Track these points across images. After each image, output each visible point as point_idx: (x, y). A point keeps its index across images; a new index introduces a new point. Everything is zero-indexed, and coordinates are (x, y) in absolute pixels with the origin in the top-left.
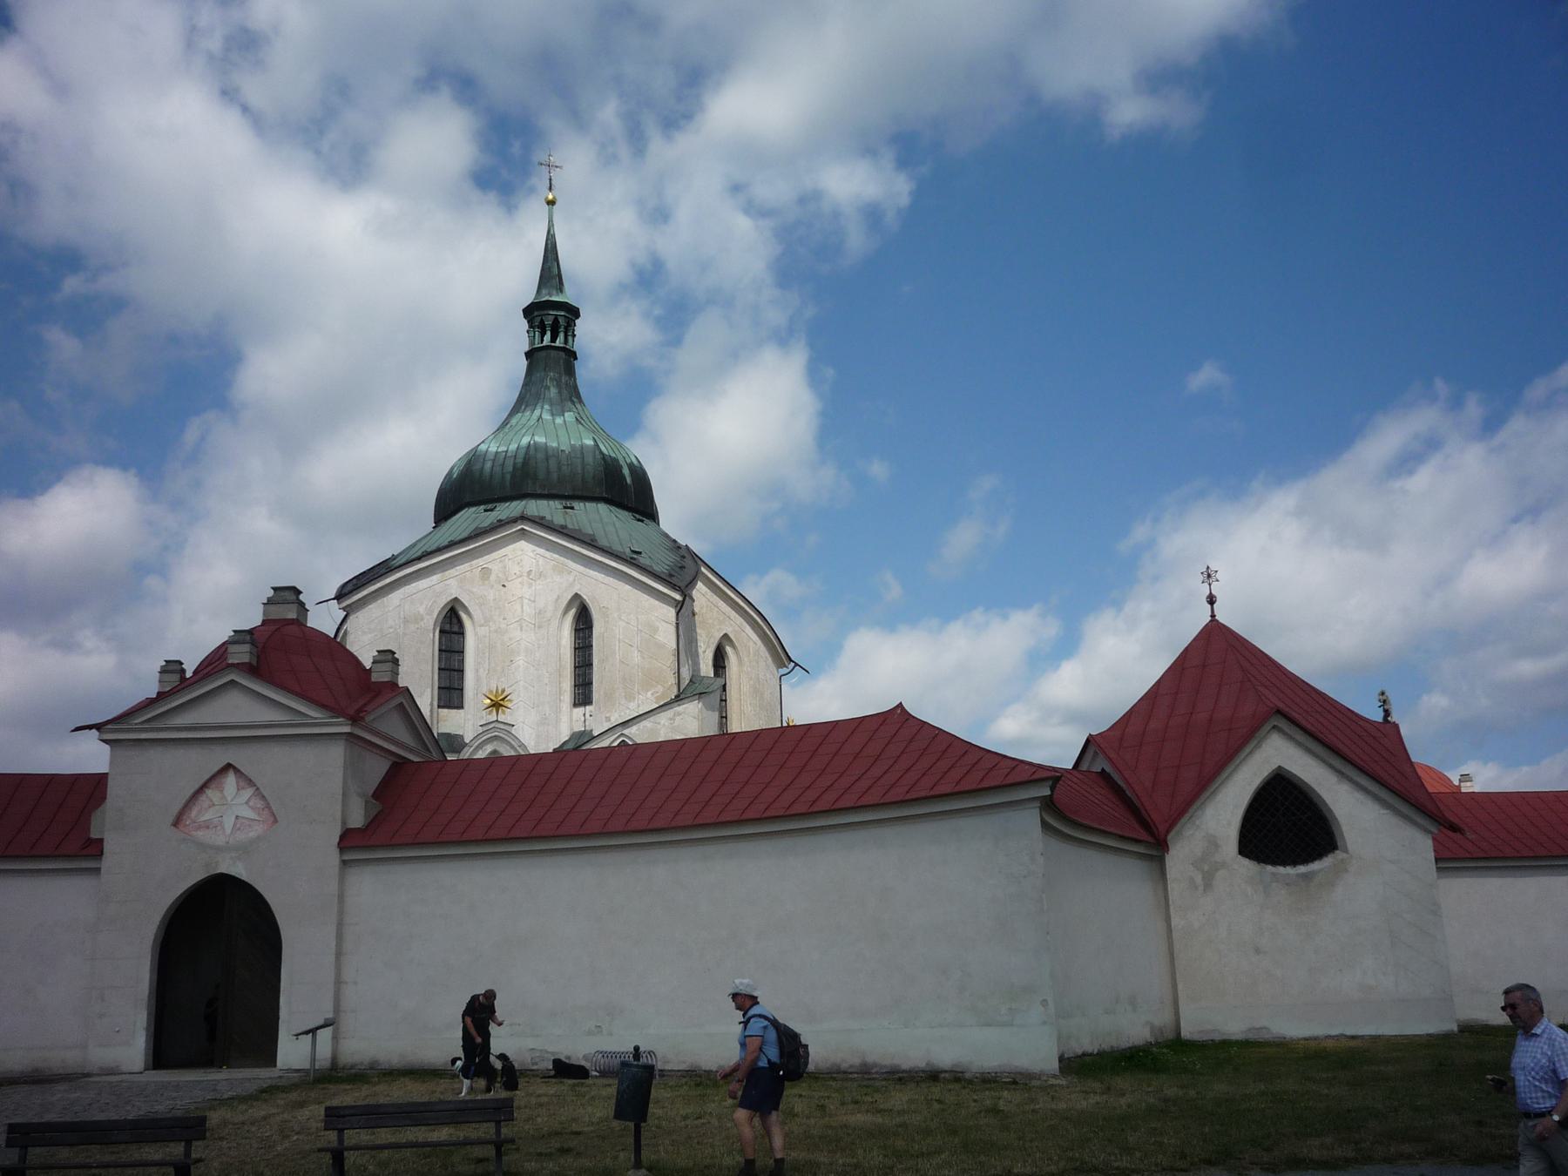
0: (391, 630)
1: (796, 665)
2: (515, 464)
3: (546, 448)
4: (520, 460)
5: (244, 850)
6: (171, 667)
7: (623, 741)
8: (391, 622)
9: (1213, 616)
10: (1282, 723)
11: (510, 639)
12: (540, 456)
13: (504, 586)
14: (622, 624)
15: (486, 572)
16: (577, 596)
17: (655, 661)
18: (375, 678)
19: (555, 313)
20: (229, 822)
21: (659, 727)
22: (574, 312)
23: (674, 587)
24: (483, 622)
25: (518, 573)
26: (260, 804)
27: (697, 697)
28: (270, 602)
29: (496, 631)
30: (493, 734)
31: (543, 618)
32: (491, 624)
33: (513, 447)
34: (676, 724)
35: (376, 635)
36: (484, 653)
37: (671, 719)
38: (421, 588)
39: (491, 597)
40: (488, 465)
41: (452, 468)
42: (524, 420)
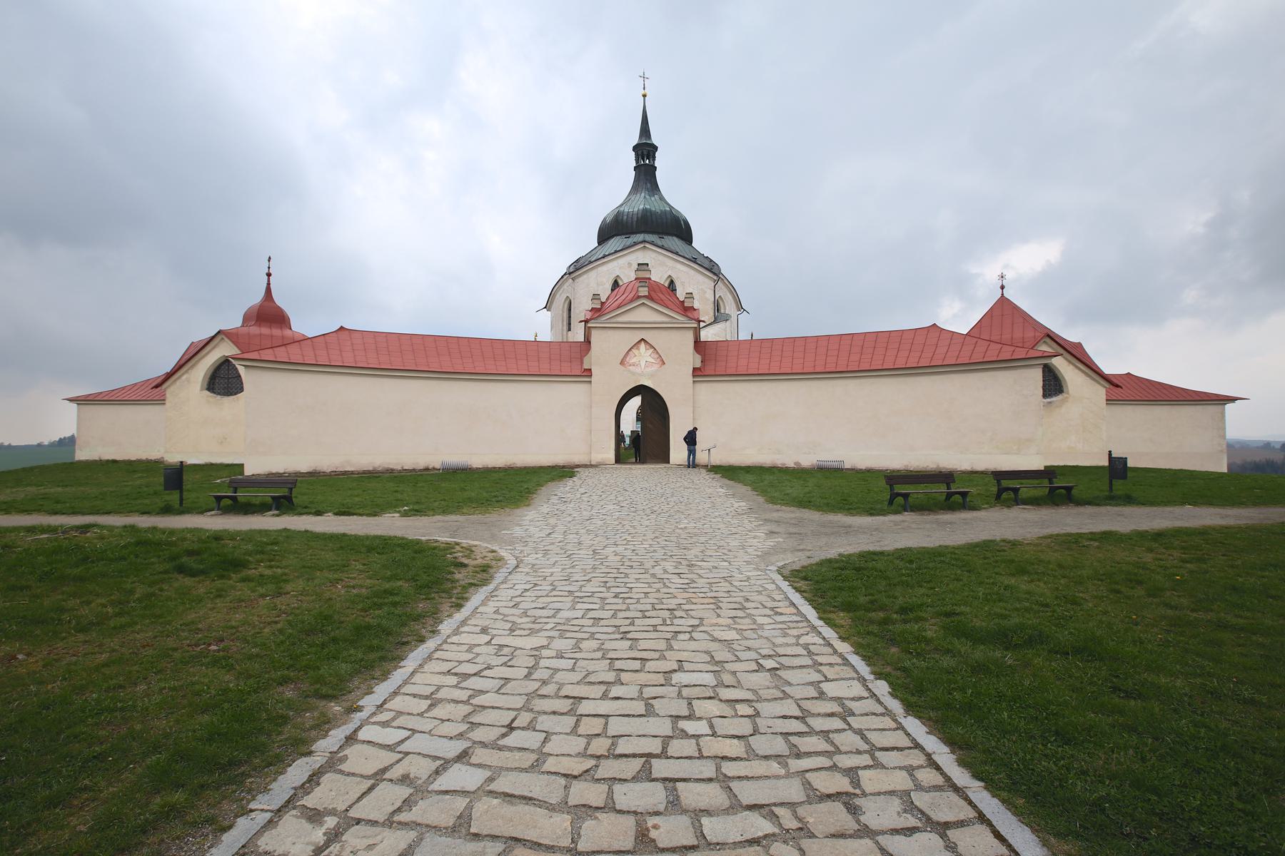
1: (744, 310)
2: (637, 218)
3: (650, 211)
4: (640, 215)
5: (652, 376)
6: (598, 297)
9: (1002, 294)
10: (1048, 340)
12: (648, 214)
16: (670, 276)
18: (686, 304)
20: (643, 364)
22: (656, 148)
23: (715, 274)
26: (656, 356)
28: (637, 270)
33: (636, 209)
40: (625, 217)
41: (605, 219)
42: (637, 198)
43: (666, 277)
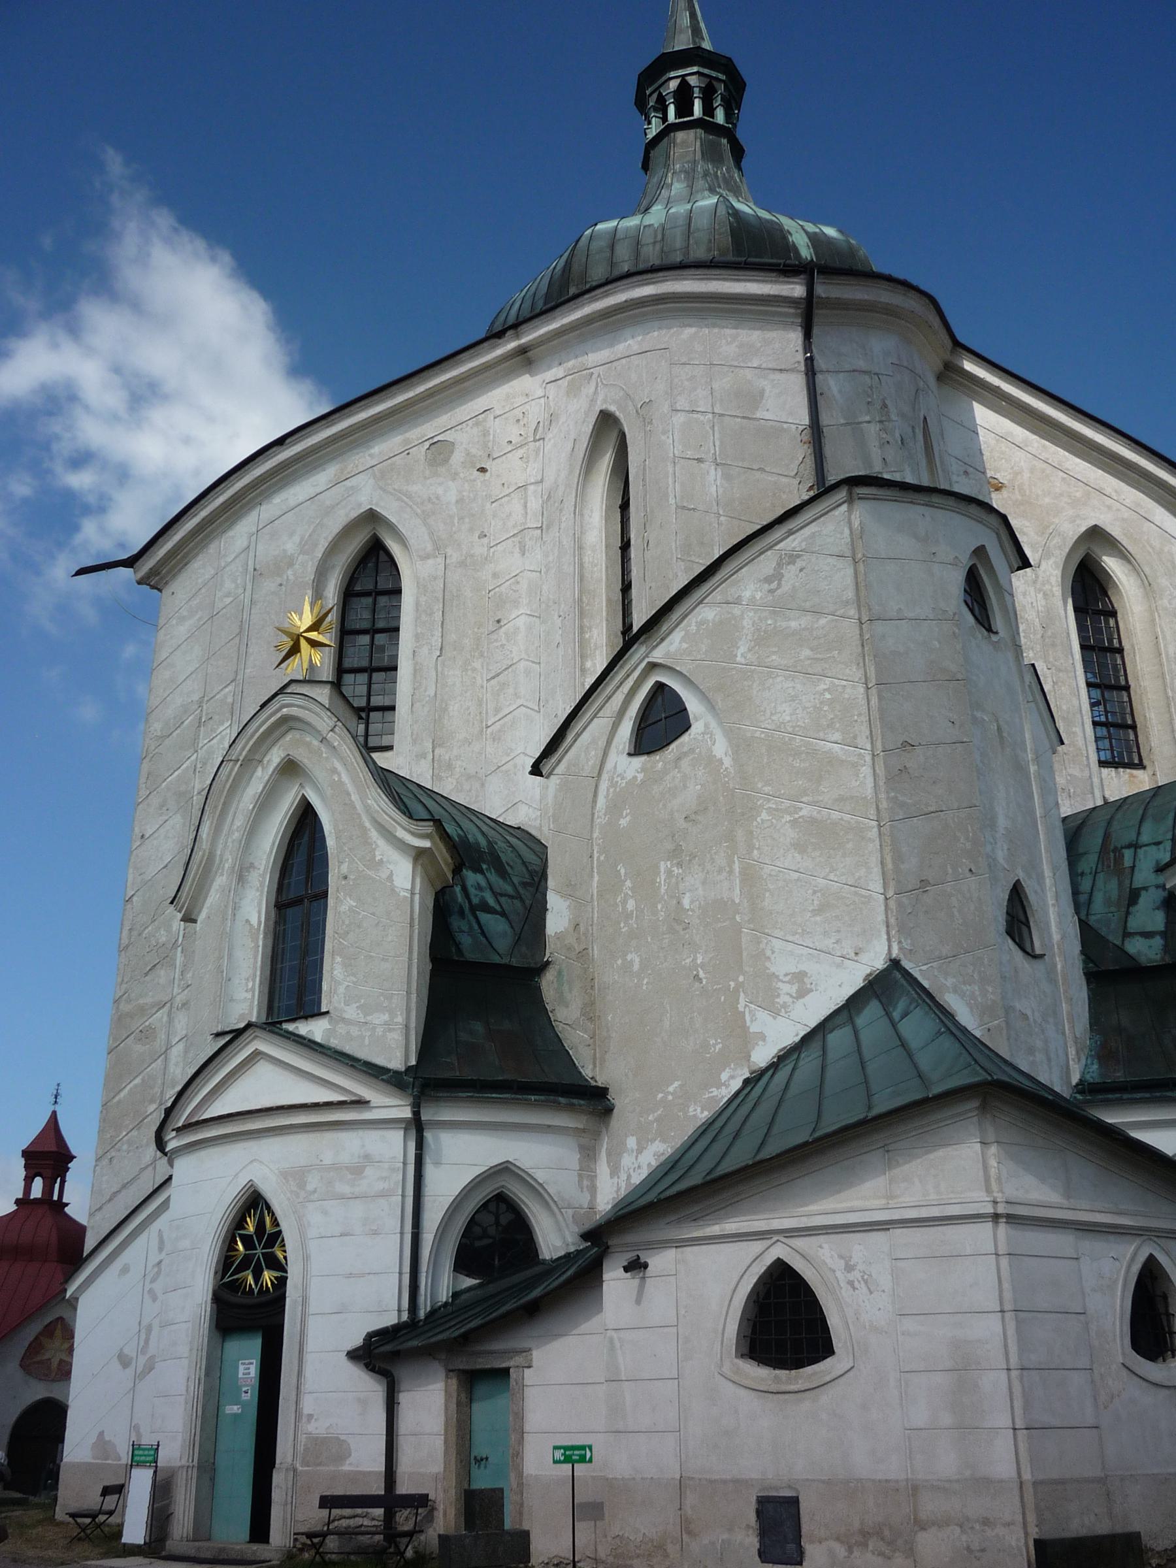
0: (228, 600)
7: (660, 687)
8: (229, 585)
11: (495, 575)
13: (483, 470)
14: (679, 419)
15: (439, 450)
17: (758, 475)
19: (681, 72)
21: (737, 610)
24: (429, 547)
25: (515, 440)
27: (842, 494)
29: (462, 564)
30: (279, 715)
31: (555, 502)
32: (449, 551)
34: (786, 587)
35: (200, 619)
36: (431, 614)
37: (768, 580)
38: (292, 502)
39: (452, 496)
43: (588, 428)
